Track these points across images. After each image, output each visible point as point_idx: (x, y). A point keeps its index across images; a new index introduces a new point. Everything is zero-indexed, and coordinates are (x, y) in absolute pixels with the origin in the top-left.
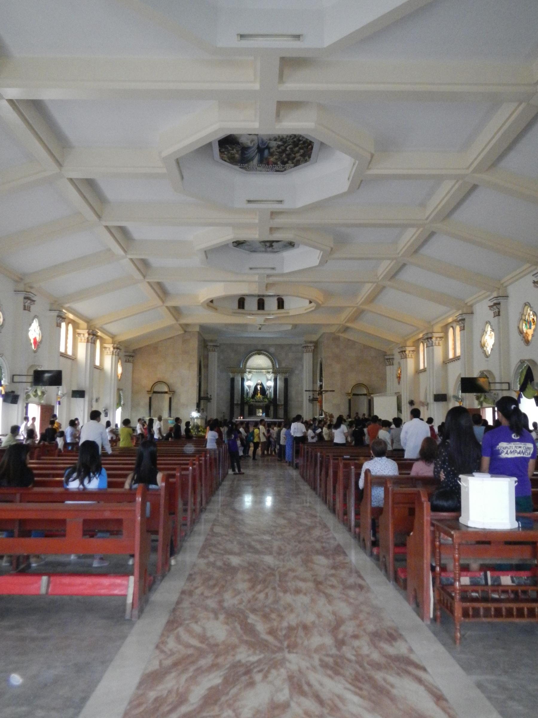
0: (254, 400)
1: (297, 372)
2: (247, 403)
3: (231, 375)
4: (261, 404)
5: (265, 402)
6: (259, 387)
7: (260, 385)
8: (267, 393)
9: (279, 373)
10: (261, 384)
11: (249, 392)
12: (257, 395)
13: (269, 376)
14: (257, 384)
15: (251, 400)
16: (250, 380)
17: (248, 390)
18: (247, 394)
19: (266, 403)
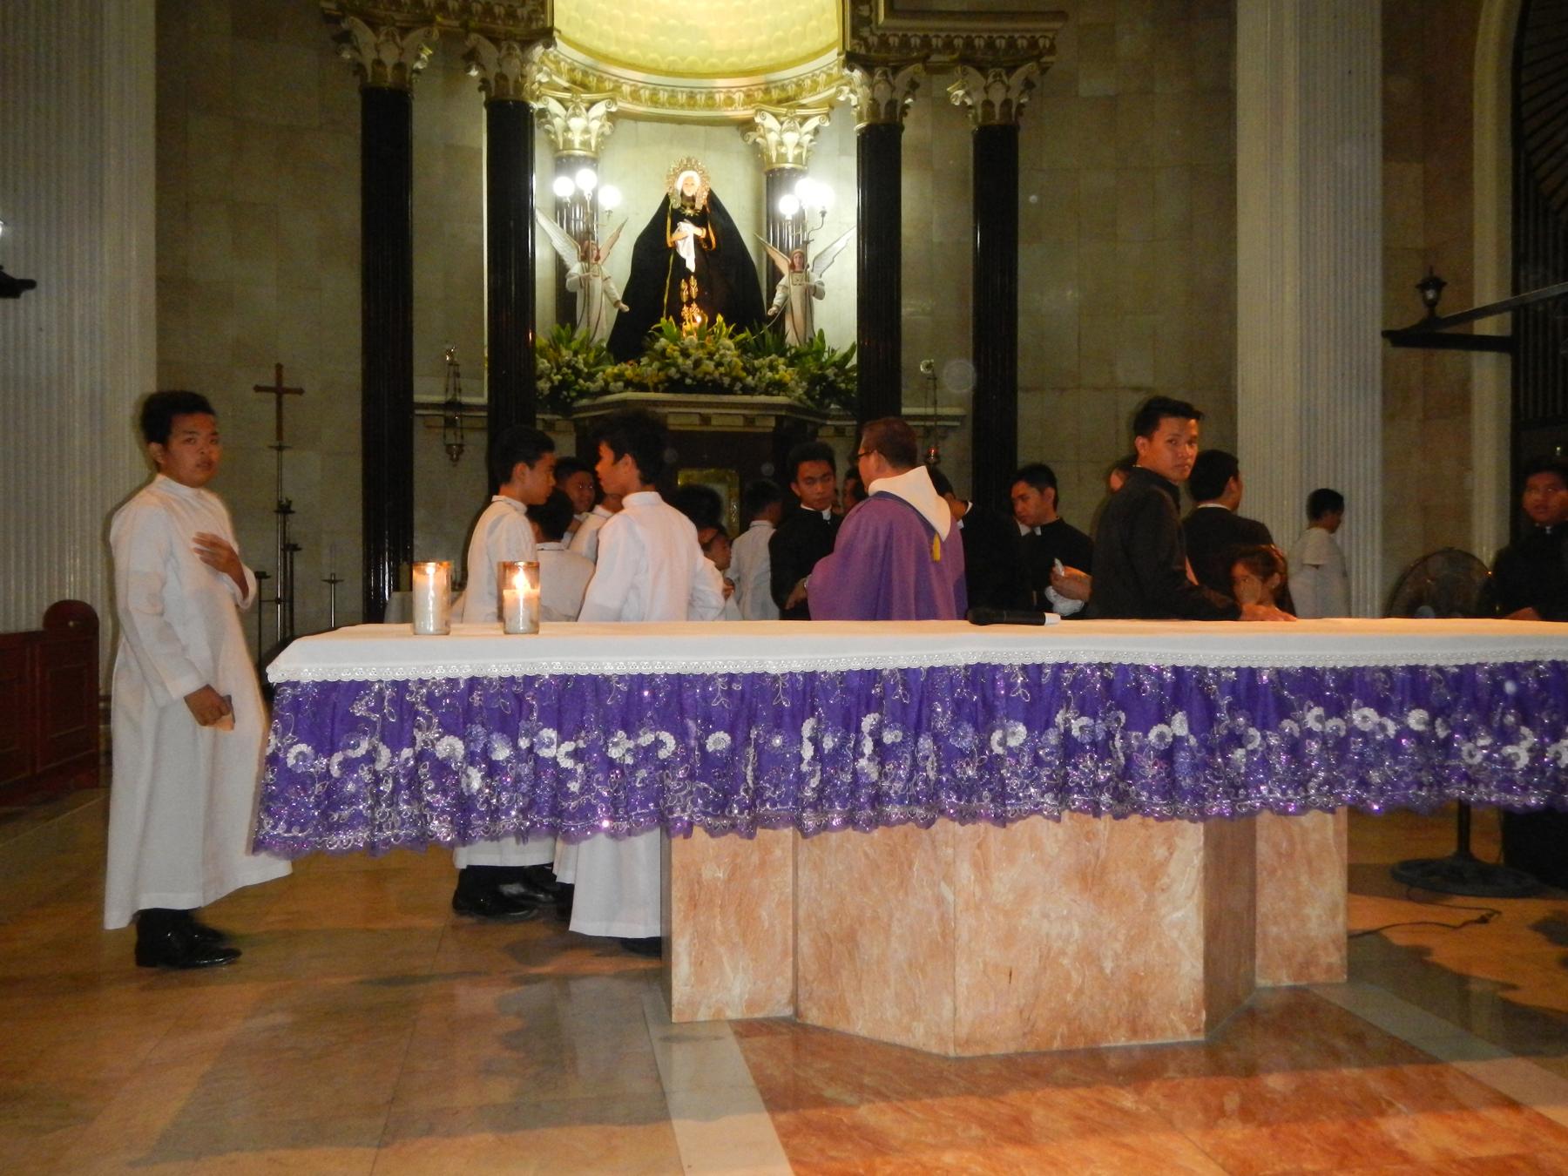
0: (647, 368)
1: (1093, 84)
2: (559, 399)
3: (368, 58)
4: (726, 414)
5: (779, 386)
6: (686, 240)
7: (699, 220)
8: (777, 301)
9: (913, 86)
10: (712, 214)
11: (585, 283)
12: (680, 320)
13: (790, 138)
14: (667, 217)
15: (611, 370)
16: (593, 161)
17: (576, 268)
18: (567, 303)
19: (781, 399)
